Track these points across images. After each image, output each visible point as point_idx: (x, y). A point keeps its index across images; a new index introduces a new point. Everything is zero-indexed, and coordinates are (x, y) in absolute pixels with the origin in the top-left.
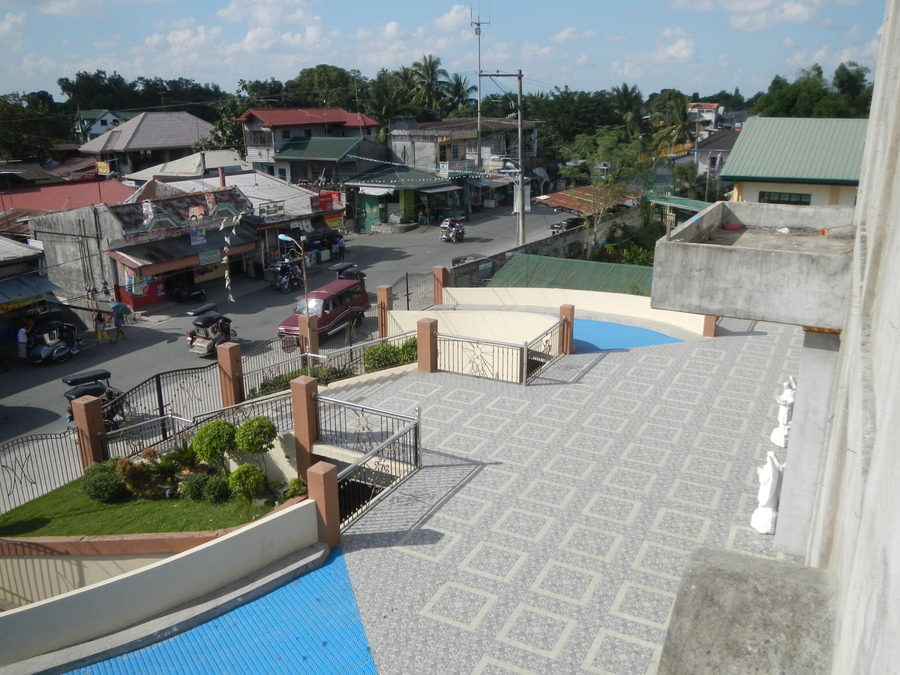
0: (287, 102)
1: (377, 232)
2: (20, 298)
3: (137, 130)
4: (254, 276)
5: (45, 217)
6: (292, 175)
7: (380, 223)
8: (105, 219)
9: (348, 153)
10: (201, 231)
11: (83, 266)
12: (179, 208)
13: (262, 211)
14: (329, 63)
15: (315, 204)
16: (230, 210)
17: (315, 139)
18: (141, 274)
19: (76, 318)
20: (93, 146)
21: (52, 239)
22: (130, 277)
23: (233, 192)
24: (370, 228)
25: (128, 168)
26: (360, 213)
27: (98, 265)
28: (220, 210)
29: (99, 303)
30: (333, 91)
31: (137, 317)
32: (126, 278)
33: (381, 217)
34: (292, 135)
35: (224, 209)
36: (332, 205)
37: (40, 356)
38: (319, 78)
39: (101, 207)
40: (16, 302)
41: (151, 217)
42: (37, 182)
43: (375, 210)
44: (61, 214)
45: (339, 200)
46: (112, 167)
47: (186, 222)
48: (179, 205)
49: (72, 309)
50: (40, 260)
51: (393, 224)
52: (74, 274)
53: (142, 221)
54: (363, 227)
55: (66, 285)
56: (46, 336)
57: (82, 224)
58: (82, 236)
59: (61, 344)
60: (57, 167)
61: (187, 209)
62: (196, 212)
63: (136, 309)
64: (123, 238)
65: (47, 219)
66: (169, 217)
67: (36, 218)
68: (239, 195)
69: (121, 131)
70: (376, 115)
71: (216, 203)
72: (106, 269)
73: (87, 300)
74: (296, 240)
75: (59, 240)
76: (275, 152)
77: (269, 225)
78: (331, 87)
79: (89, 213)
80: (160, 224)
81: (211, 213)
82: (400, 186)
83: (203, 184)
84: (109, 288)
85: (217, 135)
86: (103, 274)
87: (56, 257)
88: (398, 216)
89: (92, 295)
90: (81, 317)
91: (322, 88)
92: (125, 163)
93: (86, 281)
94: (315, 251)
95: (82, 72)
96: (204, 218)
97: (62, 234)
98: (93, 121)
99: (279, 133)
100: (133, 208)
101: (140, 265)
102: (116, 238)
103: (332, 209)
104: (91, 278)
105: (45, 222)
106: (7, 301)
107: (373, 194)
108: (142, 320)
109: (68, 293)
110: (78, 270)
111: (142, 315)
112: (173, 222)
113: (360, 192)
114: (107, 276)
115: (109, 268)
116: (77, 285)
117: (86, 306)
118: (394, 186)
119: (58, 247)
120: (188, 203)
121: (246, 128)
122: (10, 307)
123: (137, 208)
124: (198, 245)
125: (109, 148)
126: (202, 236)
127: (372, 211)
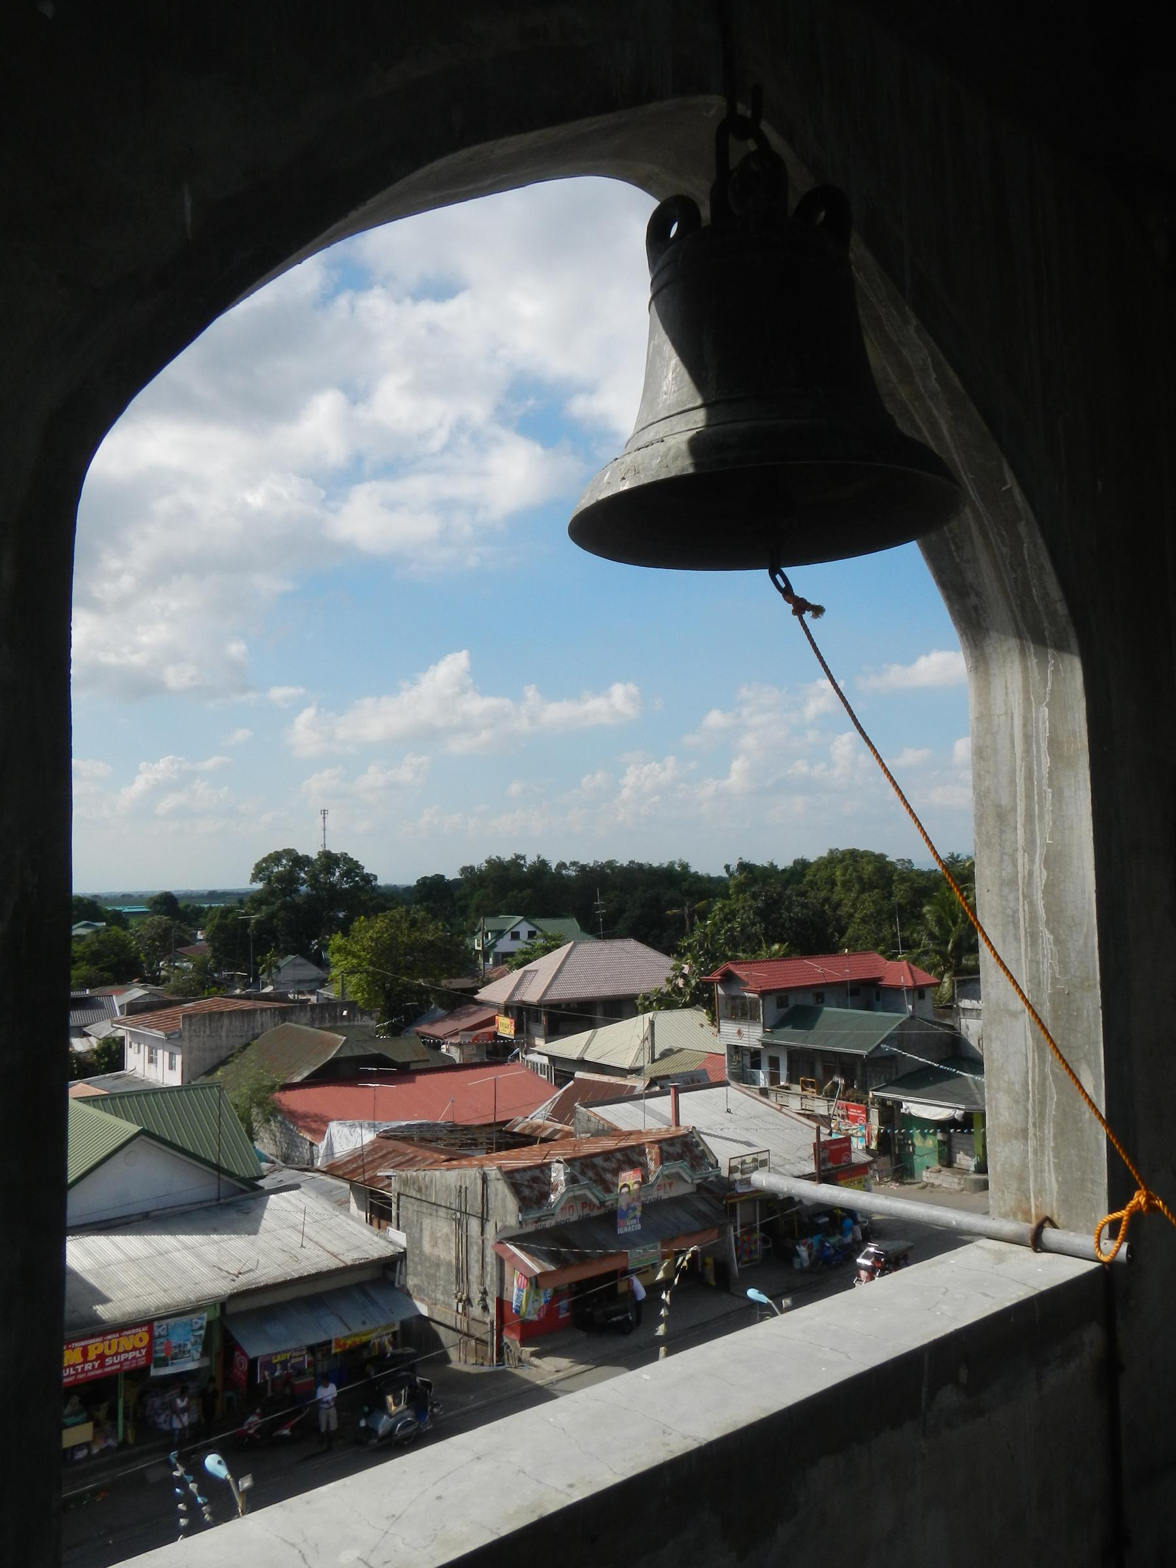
0: (791, 919)
1: (933, 1185)
2: (363, 1329)
3: (559, 970)
4: (713, 1283)
5: (415, 1173)
6: (789, 1069)
7: (938, 1167)
8: (497, 1190)
9: (883, 1042)
10: (634, 1209)
11: (457, 1258)
12: (605, 1170)
13: (732, 1170)
14: (862, 847)
15: (822, 1155)
16: (681, 1171)
17: (829, 1011)
18: (537, 1286)
19: (434, 1341)
20: (497, 992)
21: (419, 1209)
22: (519, 1289)
23: (688, 1139)
24: (922, 1176)
25: (540, 1029)
26: (903, 1146)
27: (477, 1261)
28: (666, 1172)
29: (472, 1323)
30: (866, 896)
31: (523, 1357)
32: (517, 1293)
33: (940, 1157)
34: (792, 1002)
35: (673, 1171)
36: (849, 1156)
37: (376, 1431)
38: (843, 875)
39: (493, 1173)
40: (356, 1335)
41: (562, 1189)
42: (413, 1067)
43: (931, 1142)
44: (437, 1173)
45: (867, 1121)
46: (519, 1029)
47: (612, 1196)
48: (607, 1165)
49: (433, 1324)
50: (399, 1263)
51: (964, 1172)
52: (442, 1269)
53: (546, 1196)
54: (912, 1175)
55: (429, 1283)
56: (390, 1399)
57: (463, 1195)
58: (461, 1212)
59: (408, 1412)
60: (442, 1019)
61: (616, 1172)
62: (629, 1178)
63: (524, 1342)
64: (518, 1226)
65: (417, 1176)
66: (590, 1189)
67: (403, 1174)
68: (697, 1144)
69: (536, 971)
70: (937, 952)
71: (662, 1163)
72: (489, 1269)
73: (455, 1313)
74: (776, 1304)
75: (429, 1211)
76: (764, 1032)
77: (743, 1194)
78: (863, 890)
79: (475, 1178)
80: (575, 1197)
81: (652, 1179)
82: (974, 1107)
83: (645, 1109)
84: (489, 1301)
85: (676, 985)
86: (482, 1276)
87: (421, 1237)
88: (972, 1157)
89: (464, 1308)
90: (443, 1339)
91: (850, 890)
92: (538, 1020)
93: (457, 1283)
94: (818, 1237)
95: (494, 857)
96: (640, 1189)
97: (434, 1204)
98: (500, 934)
99: (772, 1001)
100: (537, 1173)
101: (538, 1271)
102: (507, 1224)
103: (850, 1163)
104: (465, 1279)
105: (415, 1181)
106: (347, 1333)
107: (925, 1115)
108: (531, 1364)
109: (430, 1298)
110: (449, 1264)
111: (533, 1354)
112: (593, 1195)
113: (903, 1111)
114: (488, 1282)
115: (492, 1269)
116: (444, 1287)
117: (452, 1324)
118: (963, 1107)
119: (426, 1222)
120: (619, 1160)
121: (720, 991)
122: (349, 1342)
123: (542, 1172)
124: (628, 1233)
125: (517, 998)
126: (635, 1217)
127: (925, 1146)
